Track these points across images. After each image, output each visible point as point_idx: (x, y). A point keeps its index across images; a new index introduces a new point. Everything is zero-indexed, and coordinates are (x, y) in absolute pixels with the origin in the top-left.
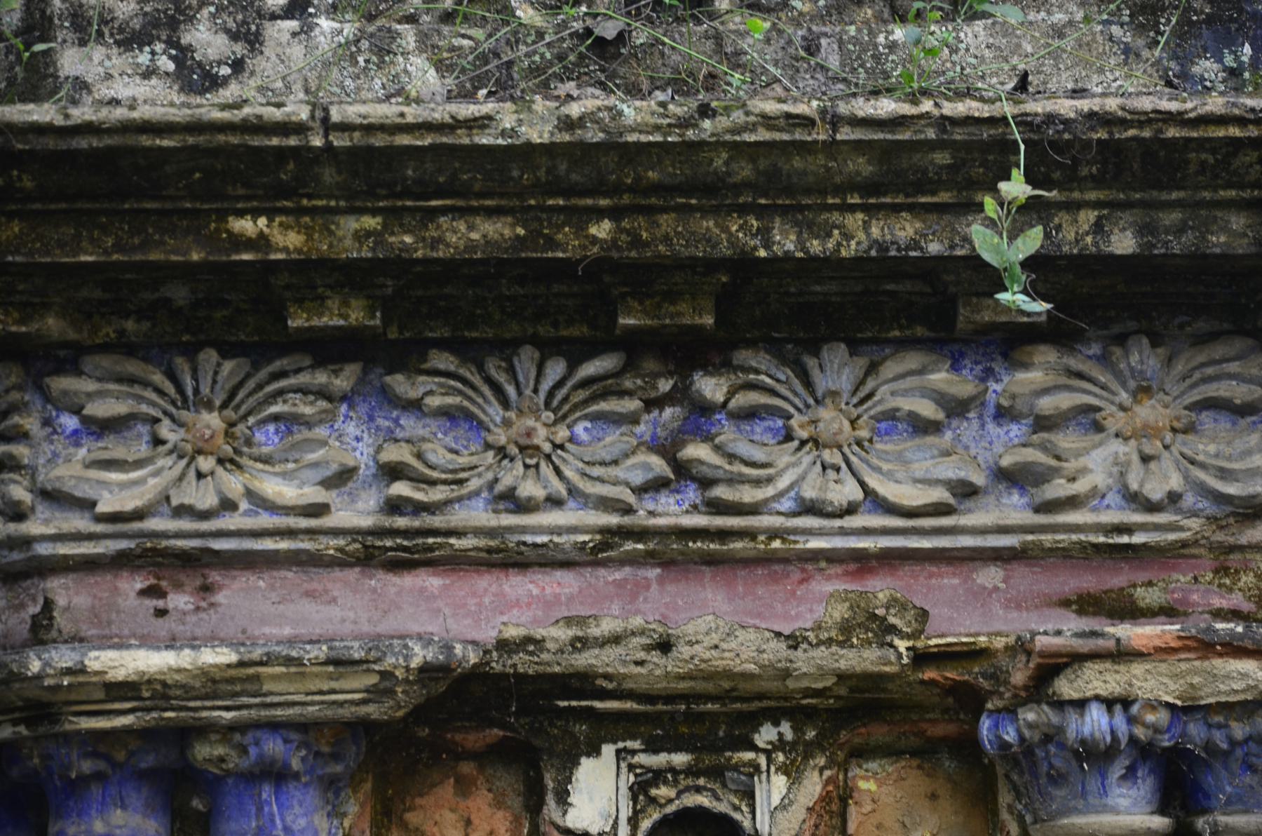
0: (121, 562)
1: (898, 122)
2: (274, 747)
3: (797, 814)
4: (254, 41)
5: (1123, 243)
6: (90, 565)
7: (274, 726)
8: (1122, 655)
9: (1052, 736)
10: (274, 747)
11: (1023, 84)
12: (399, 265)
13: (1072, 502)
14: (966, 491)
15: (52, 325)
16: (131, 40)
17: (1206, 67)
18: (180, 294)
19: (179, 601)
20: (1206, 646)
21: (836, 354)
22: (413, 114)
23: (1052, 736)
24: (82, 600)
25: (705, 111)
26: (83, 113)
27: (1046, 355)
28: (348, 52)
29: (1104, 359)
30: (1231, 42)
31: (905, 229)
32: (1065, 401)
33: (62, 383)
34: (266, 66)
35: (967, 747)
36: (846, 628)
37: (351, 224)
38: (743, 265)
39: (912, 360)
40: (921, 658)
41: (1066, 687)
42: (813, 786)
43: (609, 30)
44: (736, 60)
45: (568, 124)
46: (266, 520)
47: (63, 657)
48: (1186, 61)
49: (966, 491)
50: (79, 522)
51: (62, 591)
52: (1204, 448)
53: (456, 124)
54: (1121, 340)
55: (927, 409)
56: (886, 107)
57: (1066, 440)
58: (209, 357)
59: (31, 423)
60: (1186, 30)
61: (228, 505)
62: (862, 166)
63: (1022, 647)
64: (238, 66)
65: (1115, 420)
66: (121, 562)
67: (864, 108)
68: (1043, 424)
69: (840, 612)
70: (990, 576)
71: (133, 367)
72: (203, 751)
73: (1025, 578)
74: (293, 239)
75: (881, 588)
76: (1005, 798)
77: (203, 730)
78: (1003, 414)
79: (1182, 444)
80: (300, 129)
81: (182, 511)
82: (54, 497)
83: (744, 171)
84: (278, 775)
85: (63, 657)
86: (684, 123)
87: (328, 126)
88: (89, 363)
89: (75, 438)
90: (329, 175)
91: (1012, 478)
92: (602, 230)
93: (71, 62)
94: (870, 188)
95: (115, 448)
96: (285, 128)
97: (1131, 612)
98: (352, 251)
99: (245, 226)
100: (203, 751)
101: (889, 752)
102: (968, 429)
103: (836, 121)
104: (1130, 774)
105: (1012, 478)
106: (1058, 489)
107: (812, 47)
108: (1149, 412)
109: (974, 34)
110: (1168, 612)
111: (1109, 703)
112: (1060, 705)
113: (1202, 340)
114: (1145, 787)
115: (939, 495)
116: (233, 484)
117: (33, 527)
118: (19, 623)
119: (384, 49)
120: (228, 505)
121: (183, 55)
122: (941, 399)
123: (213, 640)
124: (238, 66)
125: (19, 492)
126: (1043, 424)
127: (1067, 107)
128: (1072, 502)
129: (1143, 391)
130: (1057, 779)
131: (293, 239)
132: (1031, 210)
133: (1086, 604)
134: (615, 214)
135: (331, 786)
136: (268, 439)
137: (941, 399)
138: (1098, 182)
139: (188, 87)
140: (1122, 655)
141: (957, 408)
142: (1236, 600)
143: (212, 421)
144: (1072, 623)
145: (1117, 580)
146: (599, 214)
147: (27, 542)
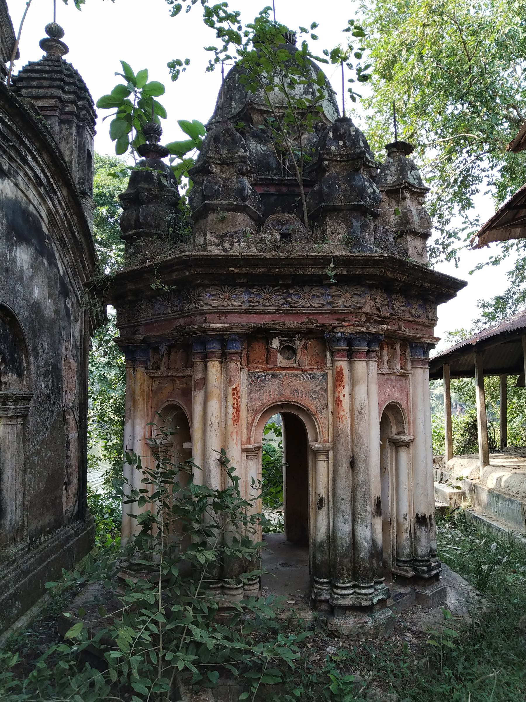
0: (215, 312)
1: (316, 256)
2: (234, 337)
3: (301, 346)
4: (233, 246)
5: (345, 273)
6: (211, 313)
7: (234, 334)
8: (343, 326)
9: (334, 337)
10: (234, 337)
11: (332, 252)
12: (251, 274)
13: (337, 307)
14: (323, 305)
15: (206, 282)
16: (217, 245)
17: (355, 250)
18: (223, 278)
19: (223, 318)
20: (354, 325)
21: (307, 287)
22: (253, 254)
23: (334, 337)
24: (210, 317)
25: (291, 254)
26: (210, 254)
27: (334, 287)
28: (245, 247)
29: (341, 288)
30: (358, 247)
31: (317, 271)
32: (336, 293)
33: (207, 289)
34: (234, 249)
35: (323, 338)
36: (307, 322)
37: (245, 269)
38: (295, 275)
39: (317, 288)
40: (317, 326)
41: (336, 330)
42: (303, 343)
43: (278, 245)
44: (295, 248)
45: (273, 256)
46: (234, 308)
47: (207, 325)
48: (352, 250)
49: (323, 305)
50: (210, 307)
51: (208, 316)
52: (354, 300)
53: (258, 256)
54: (344, 285)
55: (319, 294)
56: (315, 254)
57: (336, 298)
58: (226, 286)
59: (204, 295)
60: (353, 245)
61: (229, 305)
62: (311, 262)
63: (330, 325)
64: (231, 249)
65: (343, 296)
66: (215, 312)
67: (312, 254)
68: (333, 296)
69: (307, 320)
70: (326, 316)
71: (217, 287)
72: (225, 337)
73: (331, 316)
74: (237, 271)
75: (312, 317)
76: (327, 344)
77: (225, 334)
78: (328, 295)
79: (351, 299)
80: (238, 256)
81: (223, 306)
82: (206, 304)
83: (296, 263)
84: (235, 340)
85: (207, 325)
86: (288, 256)
87: (242, 256)
88: (211, 287)
89: (209, 297)
90: (242, 262)
91: (329, 303)
92: (277, 270)
93: (209, 248)
94: (312, 265)
95: (214, 298)
96: (236, 256)
97: (345, 321)
98: (244, 272)
99: (231, 269)
100: (225, 337)
101: (314, 338)
102: (324, 297)
103: (308, 256)
104: (344, 342)
105: (329, 303)
106: (335, 305)
107: (304, 247)
108: (347, 295)
109: (325, 246)
110: (349, 321)
111: (341, 332)
112: (335, 333)
113: (354, 286)
114: (345, 343)
115: (320, 305)
116: (229, 303)
117: (204, 308)
118: (202, 320)
119: (249, 247)
120: (229, 305)
121: (224, 247)
122: (320, 293)
123: (227, 323)
124: (231, 249)
125: (202, 304)
126: (333, 296)
127: (338, 254)
128: (337, 307)
129: (346, 292)
130: (334, 342)
131: (237, 271)
132: (334, 268)
133: (338, 320)
134: (279, 268)
135: (242, 342)
136: (234, 297)
137: (320, 293)
138: (342, 264)
139: (224, 252)
140: (343, 326)
141: (322, 294)
142: (358, 319)
143: (227, 294)
144: (337, 322)
145: (342, 317)
146: (277, 268)
147: (203, 310)
